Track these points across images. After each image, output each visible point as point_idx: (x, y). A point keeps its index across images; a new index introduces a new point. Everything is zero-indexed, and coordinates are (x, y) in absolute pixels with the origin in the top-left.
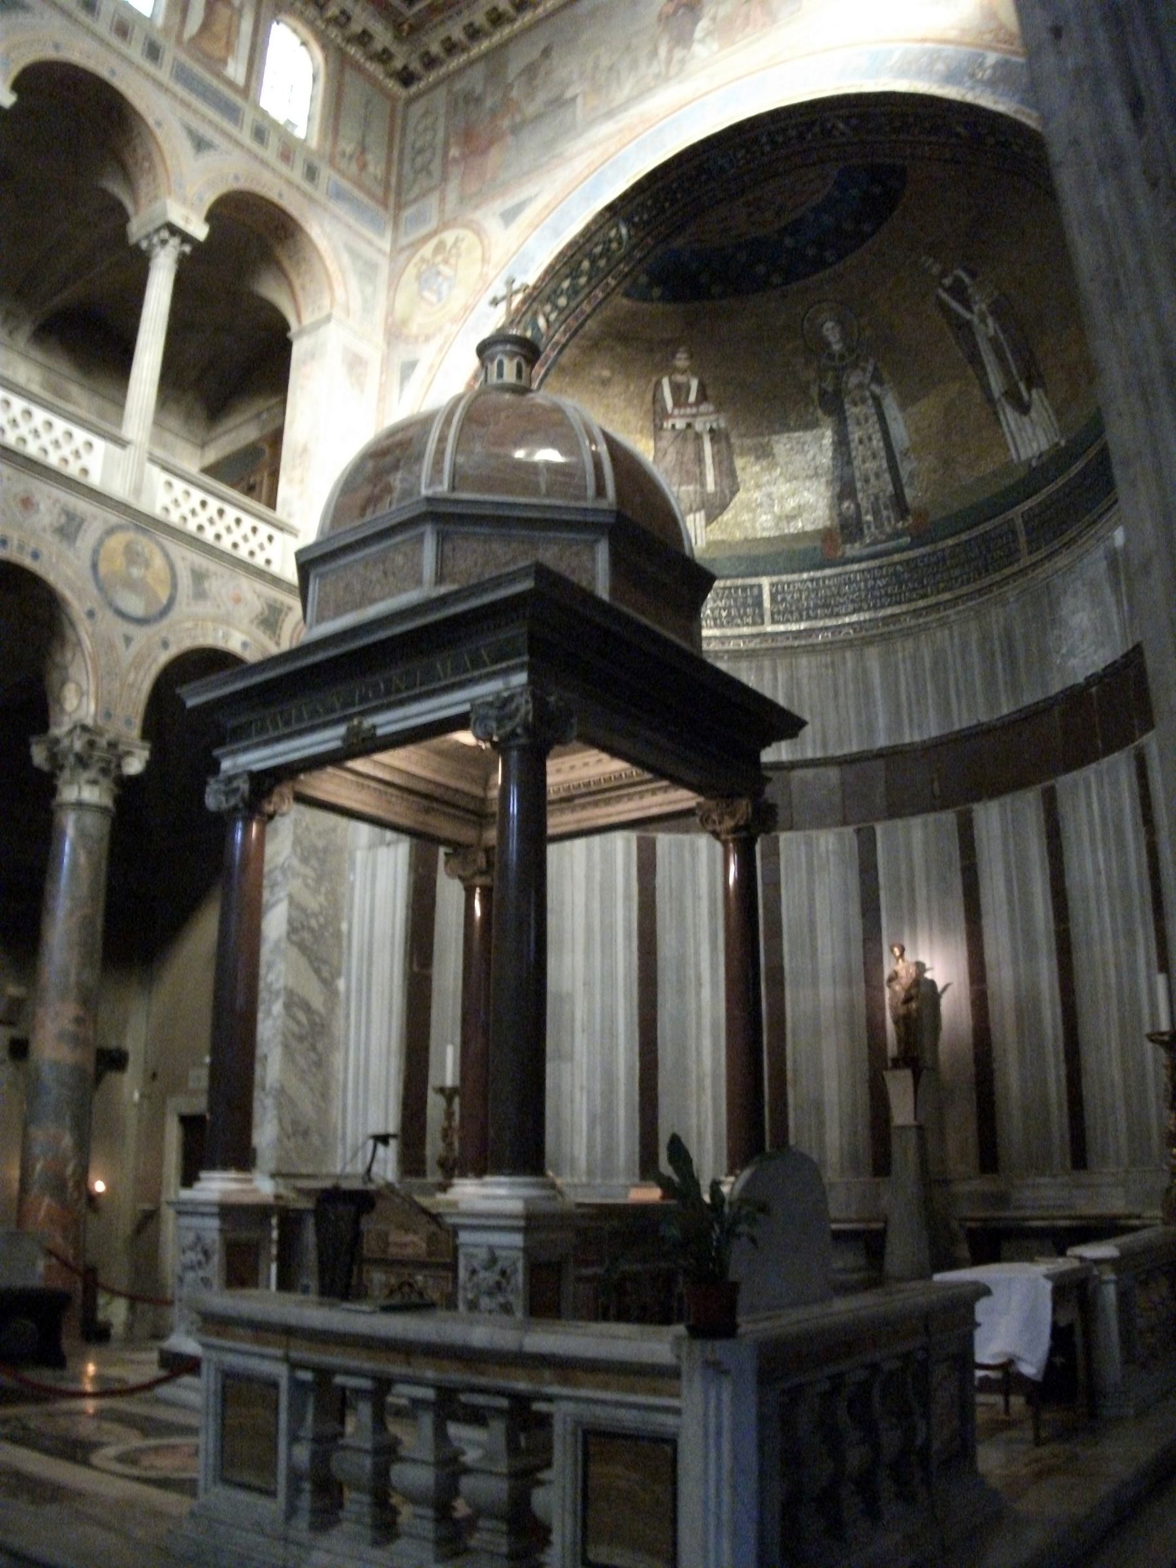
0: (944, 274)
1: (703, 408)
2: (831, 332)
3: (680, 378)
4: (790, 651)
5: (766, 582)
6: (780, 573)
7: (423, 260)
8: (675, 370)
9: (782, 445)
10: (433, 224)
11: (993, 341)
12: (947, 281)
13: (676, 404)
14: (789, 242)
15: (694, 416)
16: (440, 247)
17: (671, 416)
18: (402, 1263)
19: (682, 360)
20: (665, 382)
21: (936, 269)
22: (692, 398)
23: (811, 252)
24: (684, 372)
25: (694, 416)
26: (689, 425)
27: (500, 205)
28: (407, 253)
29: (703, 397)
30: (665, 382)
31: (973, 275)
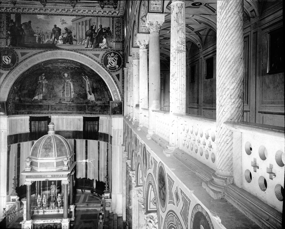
13: (41, 80)
20: (40, 77)
22: (43, 79)
30: (40, 77)
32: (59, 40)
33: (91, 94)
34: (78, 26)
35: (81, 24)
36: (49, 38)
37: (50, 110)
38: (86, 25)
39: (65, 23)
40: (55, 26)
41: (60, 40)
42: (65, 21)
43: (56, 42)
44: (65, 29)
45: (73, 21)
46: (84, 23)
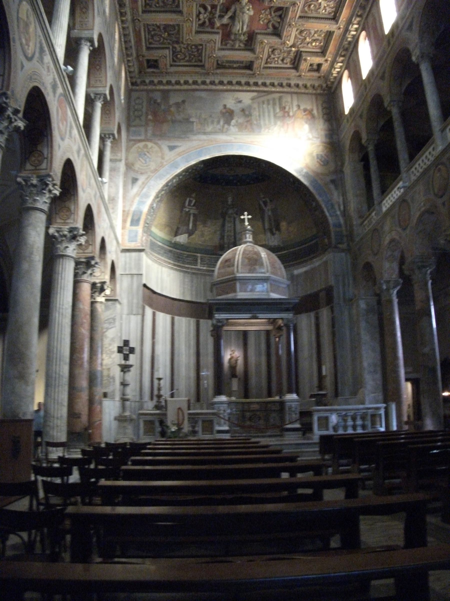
0: (264, 198)
1: (194, 208)
2: (230, 200)
3: (191, 199)
4: (205, 275)
5: (199, 255)
6: (203, 254)
7: (139, 147)
8: (191, 197)
9: (209, 223)
10: (142, 137)
11: (269, 216)
12: (264, 200)
14: (231, 178)
15: (191, 209)
16: (146, 146)
17: (186, 208)
18: (254, 411)
19: (194, 195)
20: (188, 200)
21: (262, 196)
22: (192, 204)
23: (235, 181)
24: (192, 197)
25: (191, 209)
26: (189, 211)
27: (168, 143)
28: (132, 142)
29: (194, 205)
31: (271, 201)
32: (231, 127)
33: (273, 234)
34: (261, 106)
35: (266, 102)
36: (215, 123)
37: (199, 264)
38: (274, 104)
39: (240, 102)
40: (225, 106)
41: (233, 126)
42: (241, 99)
43: (227, 129)
44: (241, 109)
45: (253, 99)
46: (271, 102)
